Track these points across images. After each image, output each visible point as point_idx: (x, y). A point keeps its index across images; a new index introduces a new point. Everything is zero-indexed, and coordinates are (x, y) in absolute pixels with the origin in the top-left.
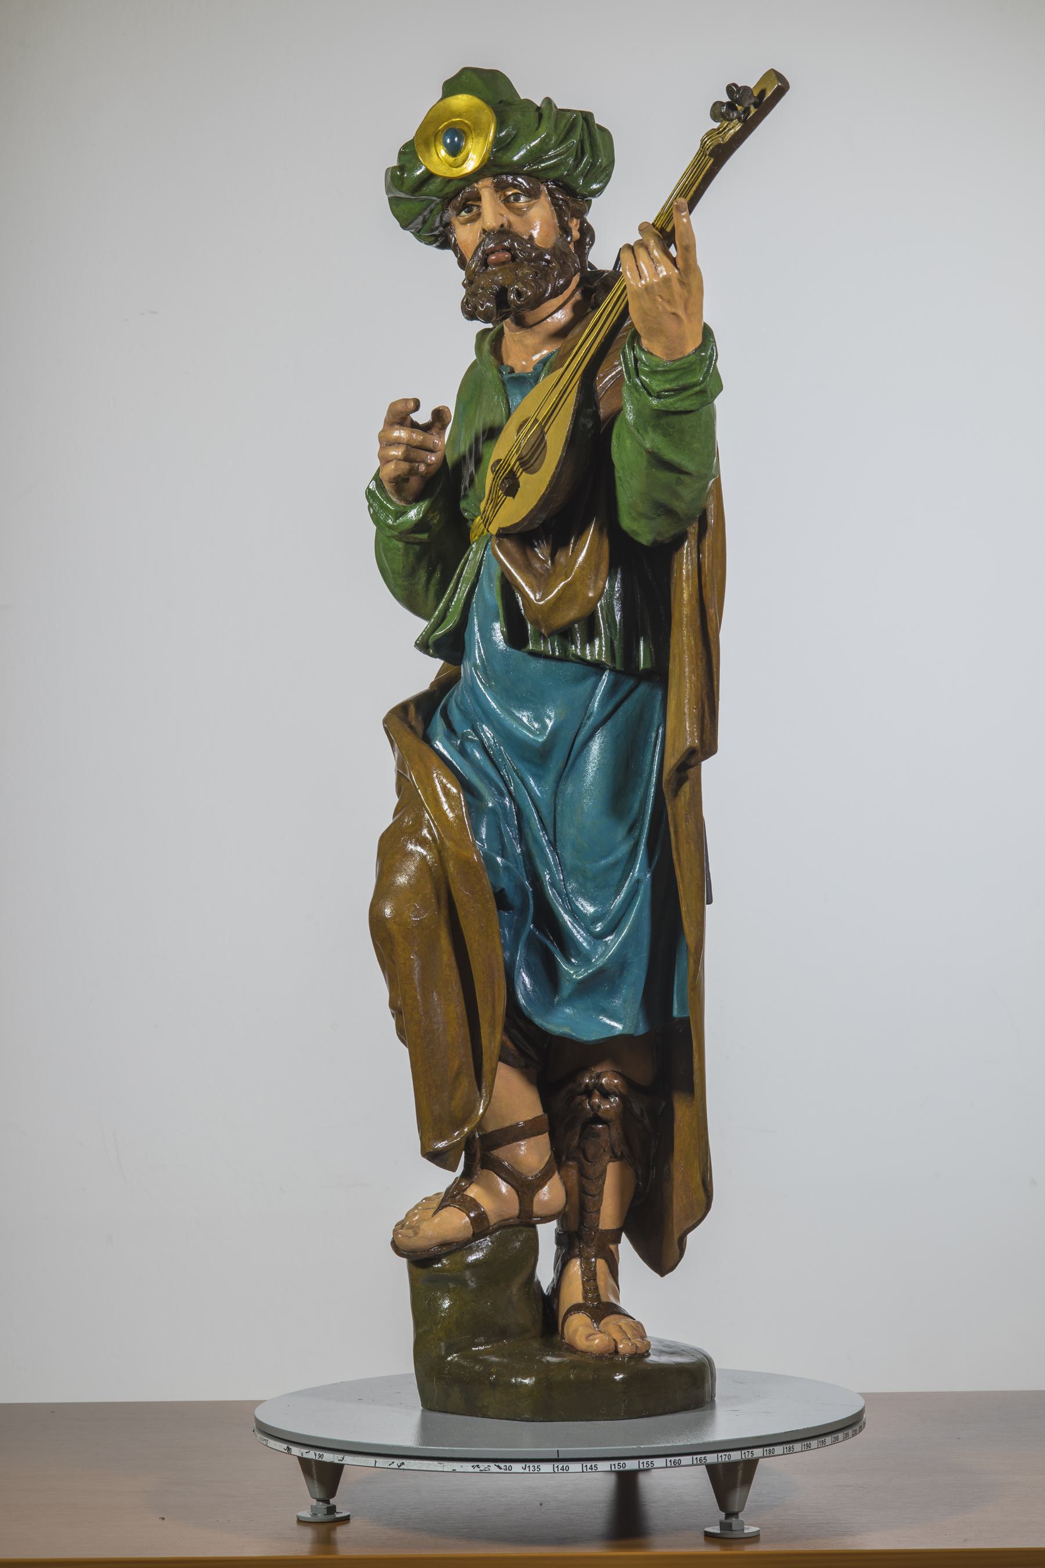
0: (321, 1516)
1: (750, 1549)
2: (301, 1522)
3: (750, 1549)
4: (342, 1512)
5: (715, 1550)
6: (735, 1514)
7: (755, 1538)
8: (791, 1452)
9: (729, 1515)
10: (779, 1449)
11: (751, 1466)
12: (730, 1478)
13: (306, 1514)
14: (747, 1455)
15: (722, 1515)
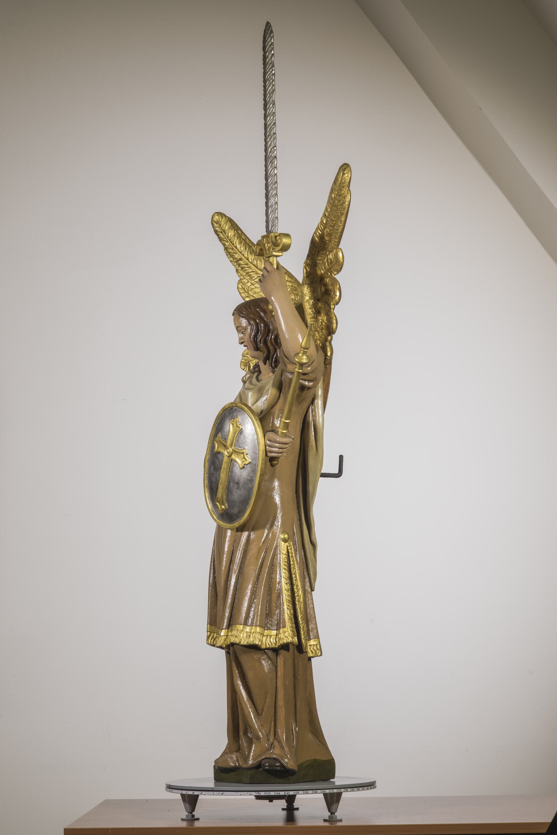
0: (190, 818)
1: (339, 824)
2: (182, 820)
3: (339, 824)
4: (196, 817)
5: (327, 824)
6: (334, 813)
7: (341, 821)
8: (353, 791)
9: (332, 814)
10: (349, 790)
11: (340, 794)
12: (332, 800)
13: (185, 817)
14: (339, 791)
15: (329, 814)
